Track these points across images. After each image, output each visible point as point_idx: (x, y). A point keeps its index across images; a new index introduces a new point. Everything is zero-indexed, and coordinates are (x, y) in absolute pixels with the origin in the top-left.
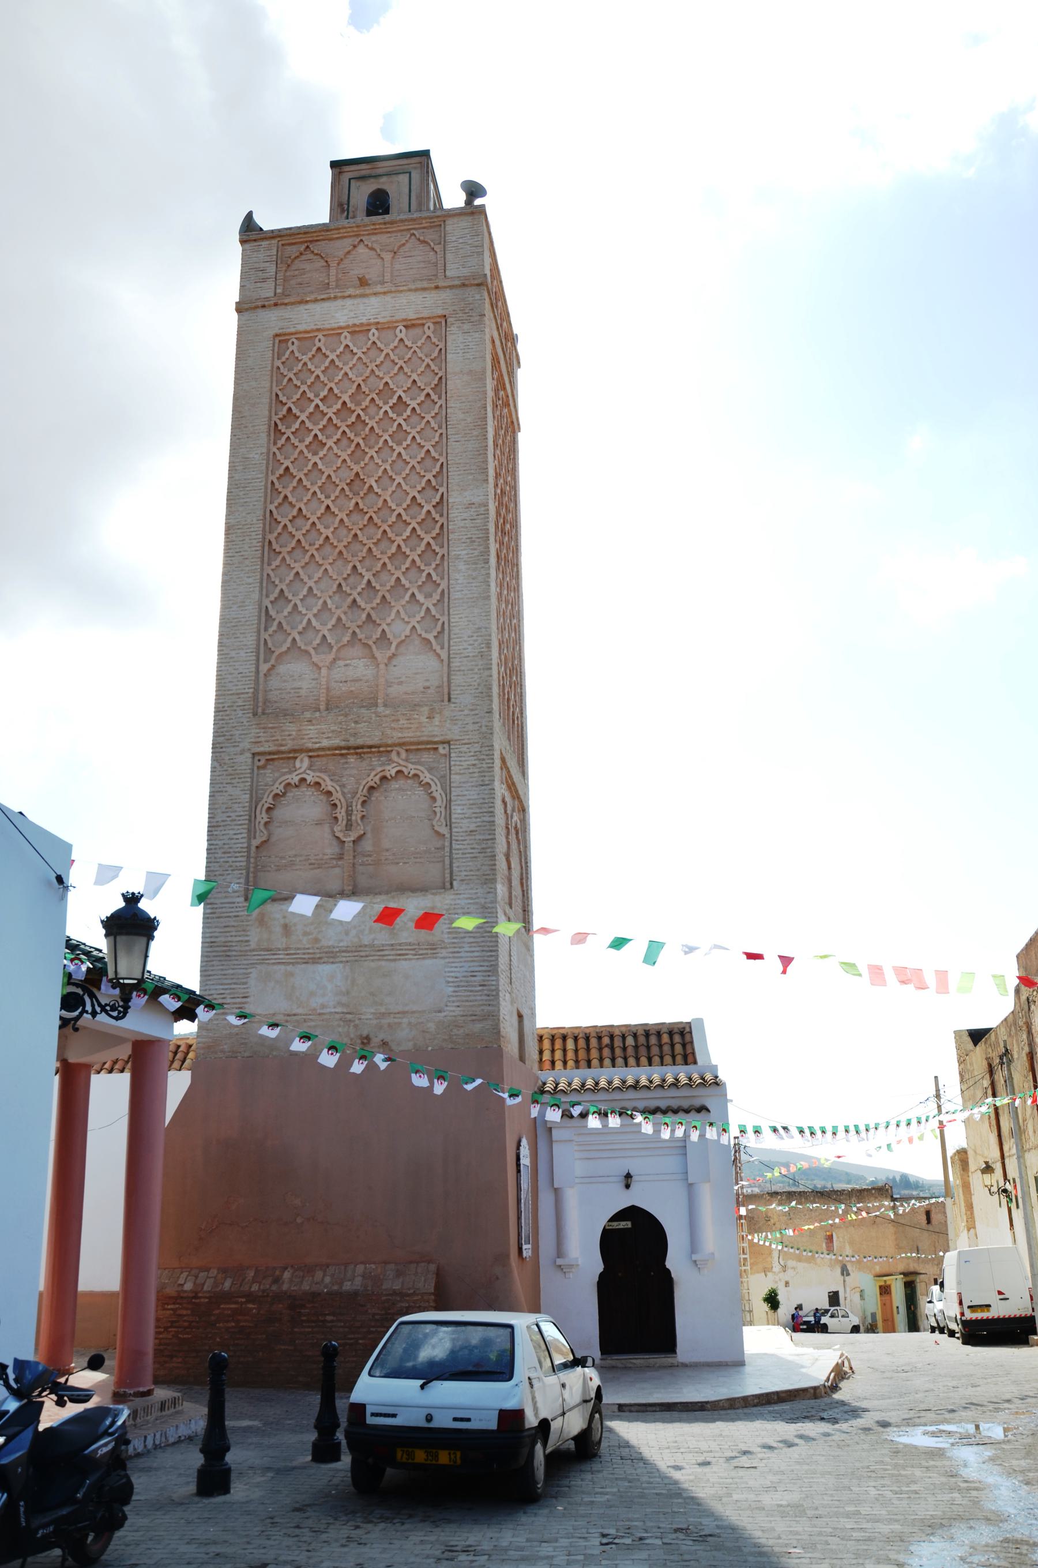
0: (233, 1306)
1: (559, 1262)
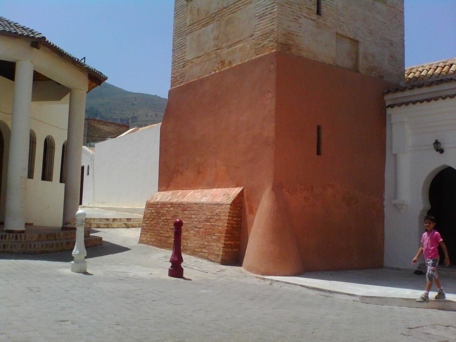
0: (166, 209)
1: (395, 202)
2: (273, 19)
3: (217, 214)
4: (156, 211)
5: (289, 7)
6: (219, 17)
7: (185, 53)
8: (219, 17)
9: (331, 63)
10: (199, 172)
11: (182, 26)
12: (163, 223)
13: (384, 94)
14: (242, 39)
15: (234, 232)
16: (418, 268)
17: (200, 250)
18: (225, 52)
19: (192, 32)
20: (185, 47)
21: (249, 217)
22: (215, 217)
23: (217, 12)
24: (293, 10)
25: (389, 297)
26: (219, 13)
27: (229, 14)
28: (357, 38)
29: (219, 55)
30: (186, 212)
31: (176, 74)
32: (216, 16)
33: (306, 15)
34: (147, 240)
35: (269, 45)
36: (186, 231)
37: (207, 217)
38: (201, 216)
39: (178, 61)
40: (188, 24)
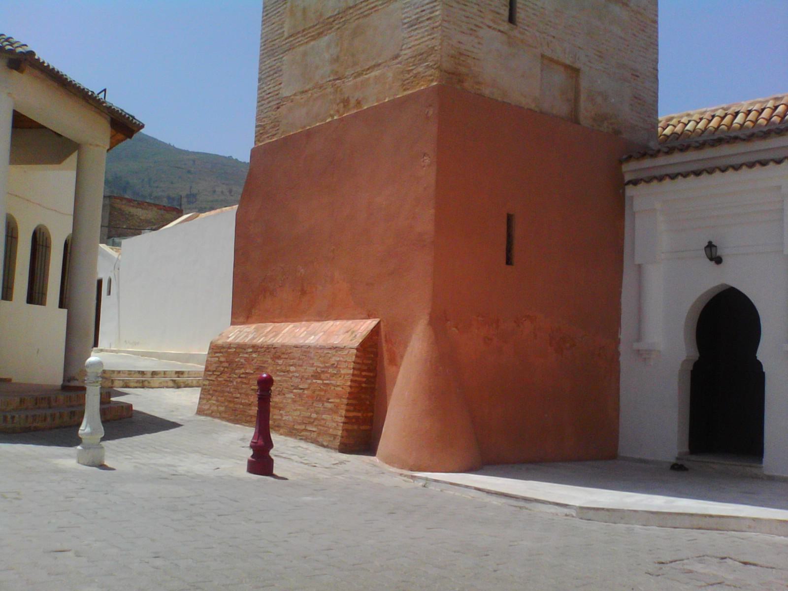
1: (636, 346)
2: (433, 28)
3: (334, 364)
4: (226, 359)
5: (461, 9)
6: (340, 23)
7: (280, 84)
8: (340, 23)
9: (533, 106)
10: (303, 292)
11: (276, 38)
12: (239, 380)
13: (621, 162)
14: (380, 61)
15: (363, 396)
16: (678, 459)
17: (303, 427)
18: (350, 83)
19: (294, 48)
20: (281, 73)
21: (389, 370)
22: (330, 370)
23: (336, 15)
24: (468, 14)
25: (626, 508)
26: (340, 16)
27: (357, 19)
28: (577, 65)
29: (339, 89)
30: (280, 362)
31: (264, 121)
32: (334, 21)
33: (491, 24)
34: (212, 408)
35: (426, 74)
36: (279, 394)
37: (316, 369)
38: (306, 369)
39: (268, 98)
40: (286, 35)
